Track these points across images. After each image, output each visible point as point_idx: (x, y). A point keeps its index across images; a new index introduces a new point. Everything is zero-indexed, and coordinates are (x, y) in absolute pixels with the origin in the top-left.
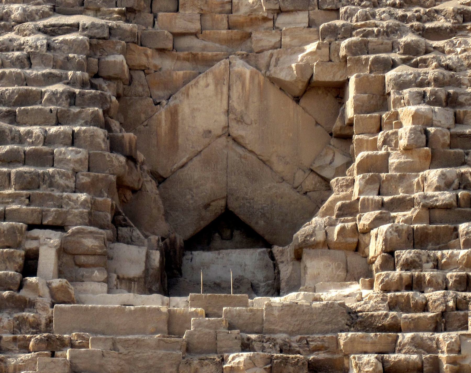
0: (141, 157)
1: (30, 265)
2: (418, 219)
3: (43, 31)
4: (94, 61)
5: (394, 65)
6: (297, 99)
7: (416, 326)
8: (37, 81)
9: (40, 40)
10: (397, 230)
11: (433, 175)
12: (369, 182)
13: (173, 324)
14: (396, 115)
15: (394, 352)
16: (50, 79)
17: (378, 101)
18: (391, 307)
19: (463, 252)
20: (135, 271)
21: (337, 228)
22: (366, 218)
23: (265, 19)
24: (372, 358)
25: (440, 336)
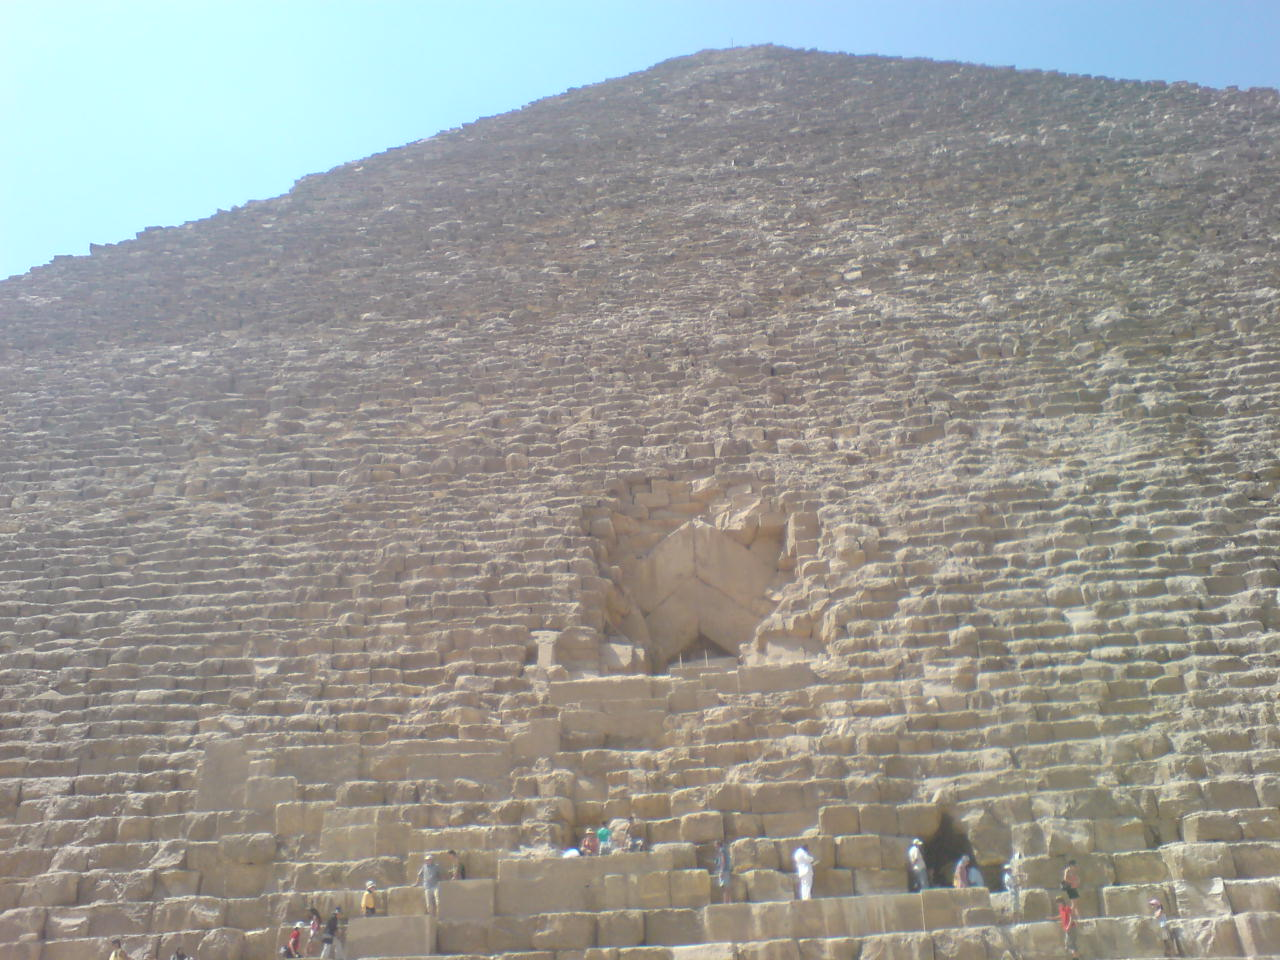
0: (627, 590)
1: (531, 656)
2: (862, 599)
3: (547, 505)
4: (586, 523)
5: (822, 505)
6: (748, 547)
7: (877, 677)
8: (539, 533)
9: (546, 509)
10: (846, 607)
11: (871, 568)
12: (816, 582)
13: (656, 690)
14: (830, 535)
15: (859, 698)
16: (550, 532)
17: (812, 529)
18: (852, 663)
19: (906, 620)
20: (625, 661)
21: (794, 617)
22: (817, 606)
23: (717, 492)
24: (842, 704)
25: (902, 682)
